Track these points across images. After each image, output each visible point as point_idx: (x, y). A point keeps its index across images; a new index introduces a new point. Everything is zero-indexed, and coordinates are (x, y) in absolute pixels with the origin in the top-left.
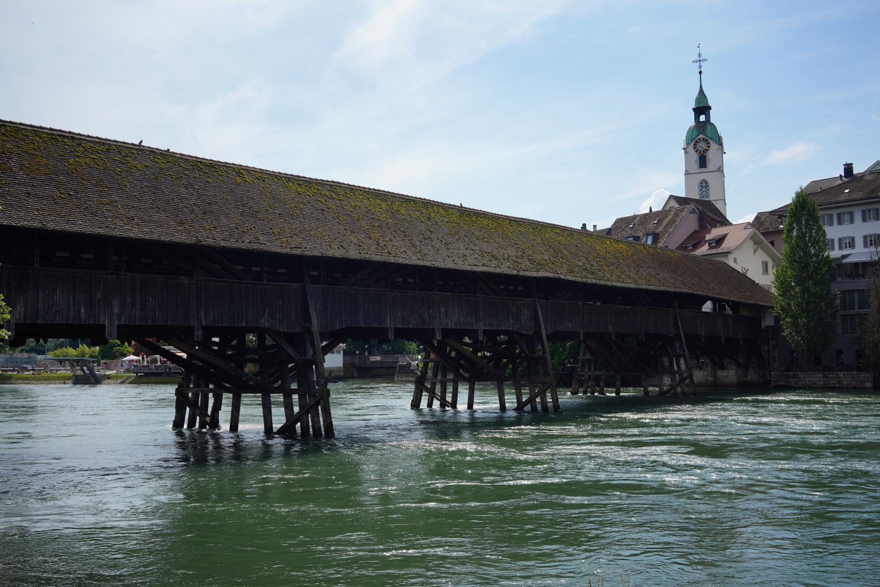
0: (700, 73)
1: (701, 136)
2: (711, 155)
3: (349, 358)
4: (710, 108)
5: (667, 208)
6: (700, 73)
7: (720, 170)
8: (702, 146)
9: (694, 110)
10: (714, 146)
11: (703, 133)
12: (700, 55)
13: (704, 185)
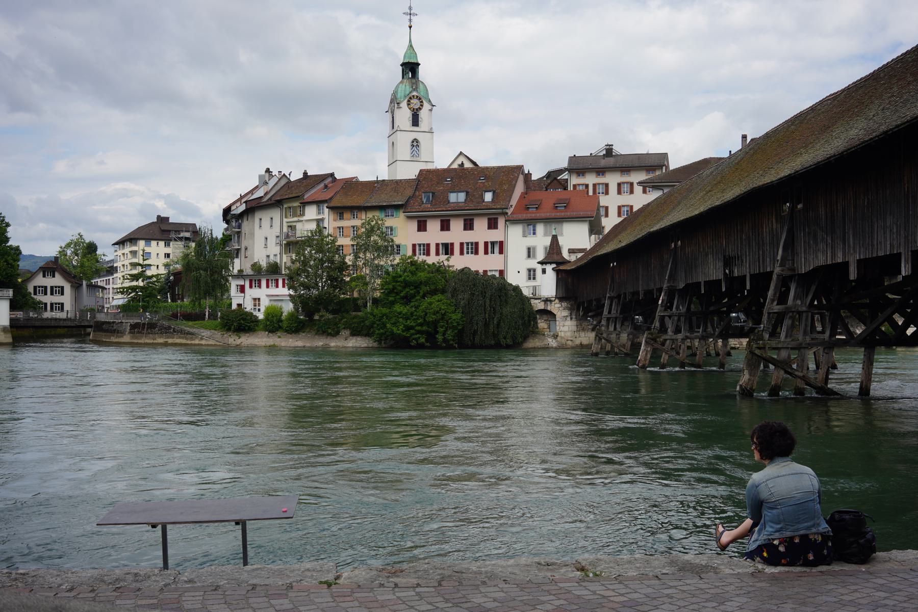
0: (410, 27)
1: (415, 93)
2: (423, 114)
3: (20, 314)
4: (419, 64)
5: (455, 166)
6: (410, 27)
7: (431, 132)
8: (415, 103)
9: (402, 65)
10: (426, 104)
11: (416, 89)
12: (410, 8)
13: (415, 144)
